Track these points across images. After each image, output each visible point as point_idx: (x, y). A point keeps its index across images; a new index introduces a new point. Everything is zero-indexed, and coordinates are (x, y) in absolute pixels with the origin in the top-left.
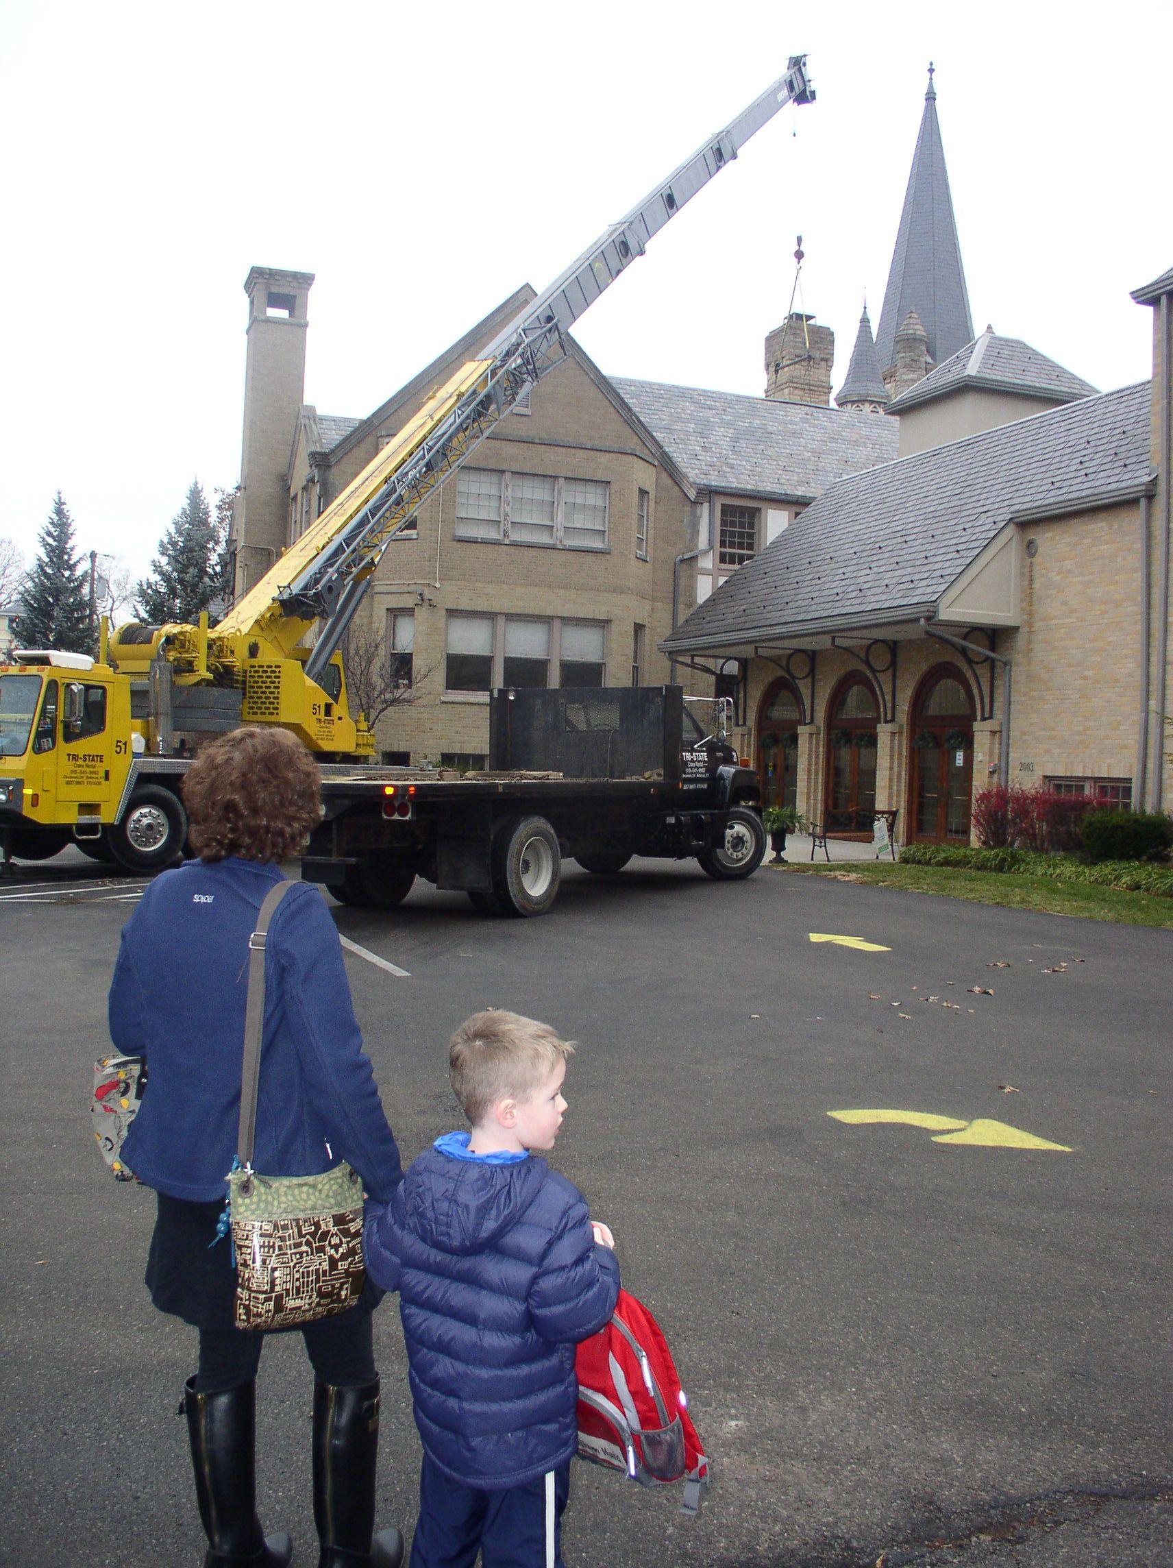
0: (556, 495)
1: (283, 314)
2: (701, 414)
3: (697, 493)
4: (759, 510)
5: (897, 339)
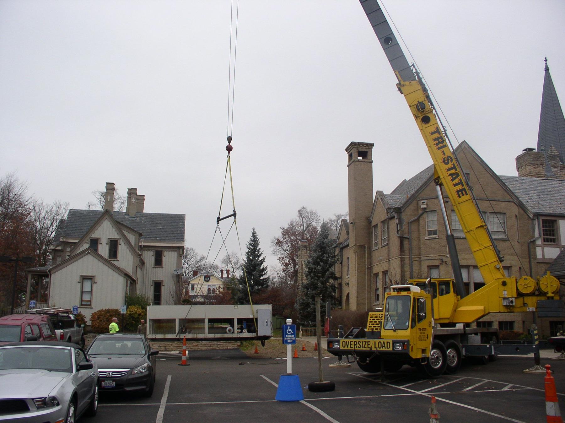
0: (505, 220)
1: (360, 158)
2: (523, 186)
3: (534, 215)
4: (556, 221)
5: (547, 156)
